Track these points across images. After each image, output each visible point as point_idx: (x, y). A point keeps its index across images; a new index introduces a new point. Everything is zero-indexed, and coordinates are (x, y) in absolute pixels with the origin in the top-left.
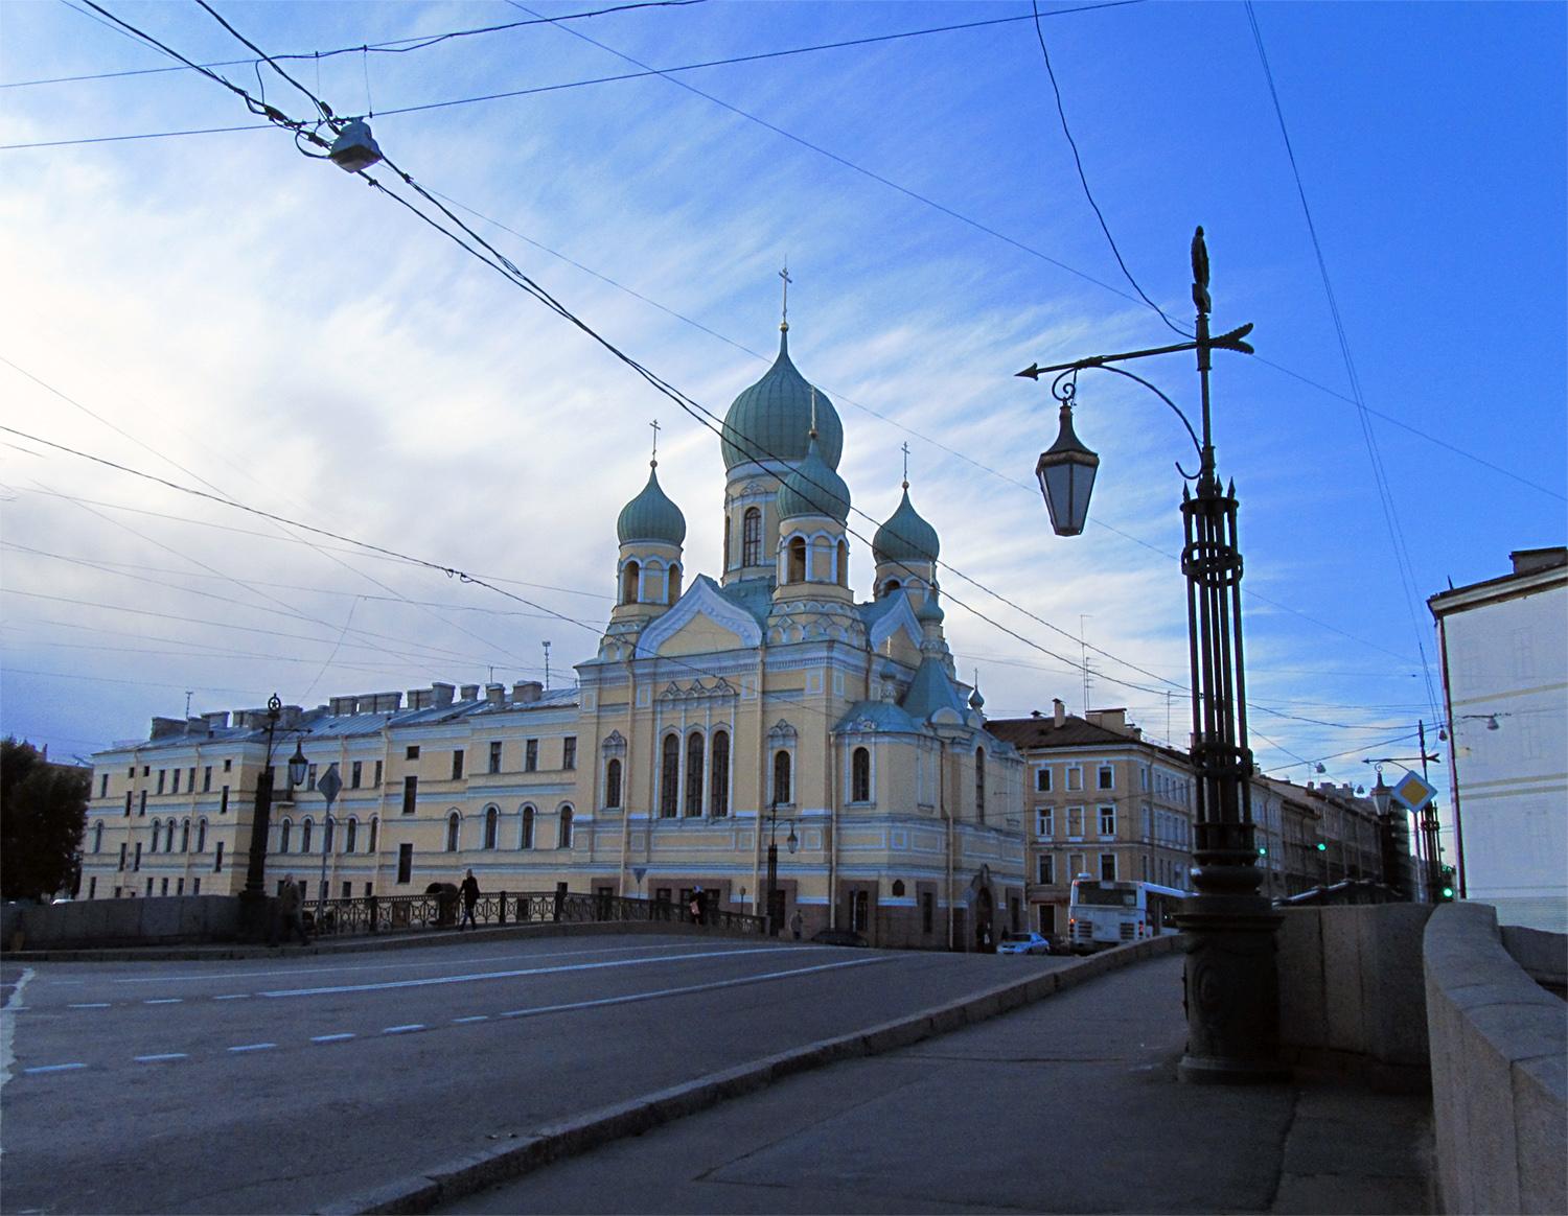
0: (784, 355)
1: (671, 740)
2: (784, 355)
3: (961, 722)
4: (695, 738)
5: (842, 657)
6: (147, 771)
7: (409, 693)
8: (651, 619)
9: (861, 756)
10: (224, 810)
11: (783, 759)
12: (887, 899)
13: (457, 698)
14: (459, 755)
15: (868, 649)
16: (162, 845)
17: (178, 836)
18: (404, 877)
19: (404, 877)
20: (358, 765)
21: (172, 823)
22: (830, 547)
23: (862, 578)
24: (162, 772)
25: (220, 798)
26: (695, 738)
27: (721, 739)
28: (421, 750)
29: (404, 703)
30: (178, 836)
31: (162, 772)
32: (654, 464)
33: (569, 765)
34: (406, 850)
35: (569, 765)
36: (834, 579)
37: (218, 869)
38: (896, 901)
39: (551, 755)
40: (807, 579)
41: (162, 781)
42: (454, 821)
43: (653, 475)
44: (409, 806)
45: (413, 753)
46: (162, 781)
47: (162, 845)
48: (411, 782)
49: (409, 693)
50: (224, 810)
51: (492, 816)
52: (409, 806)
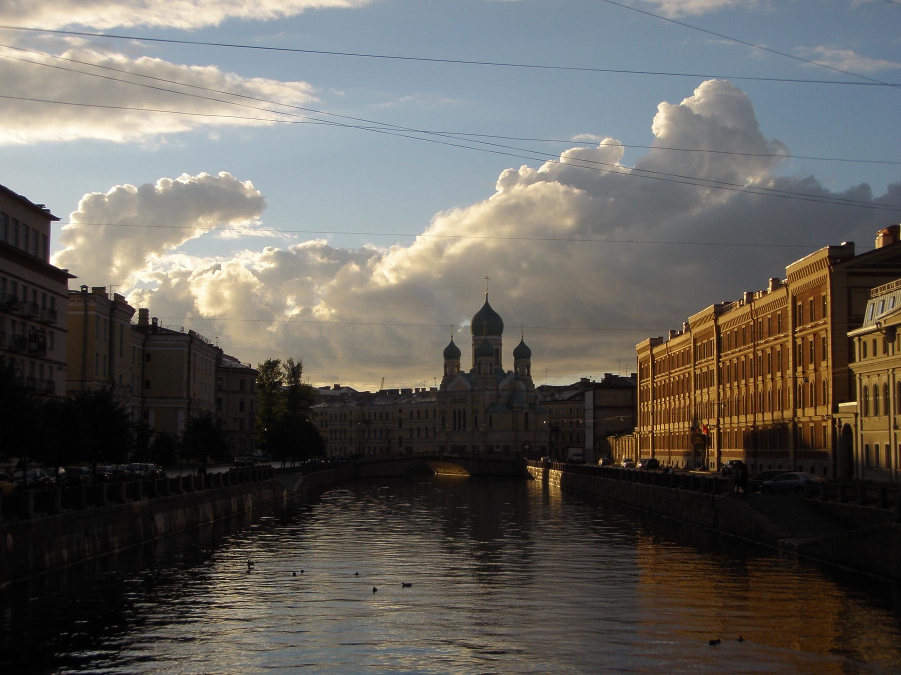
0: (487, 303)
1: (455, 412)
2: (487, 303)
3: (520, 406)
4: (459, 412)
5: (489, 393)
6: (326, 414)
7: (401, 389)
8: (451, 380)
9: (491, 418)
10: (351, 426)
11: (476, 417)
12: (496, 450)
13: (414, 392)
14: (411, 412)
15: (497, 390)
16: (334, 437)
17: (338, 434)
18: (400, 446)
19: (400, 446)
20: (387, 413)
21: (336, 430)
22: (488, 365)
23: (508, 365)
24: (331, 414)
25: (349, 423)
26: (459, 412)
27: (464, 412)
28: (403, 410)
29: (400, 393)
30: (338, 434)
31: (331, 414)
32: (452, 336)
33: (435, 417)
34: (400, 438)
35: (435, 417)
36: (488, 373)
37: (351, 444)
38: (499, 450)
39: (431, 415)
40: (482, 373)
41: (331, 417)
42: (411, 430)
43: (452, 339)
44: (400, 426)
45: (400, 411)
46: (331, 417)
47: (334, 437)
48: (400, 419)
49: (401, 389)
50: (351, 426)
51: (419, 429)
52: (400, 426)
